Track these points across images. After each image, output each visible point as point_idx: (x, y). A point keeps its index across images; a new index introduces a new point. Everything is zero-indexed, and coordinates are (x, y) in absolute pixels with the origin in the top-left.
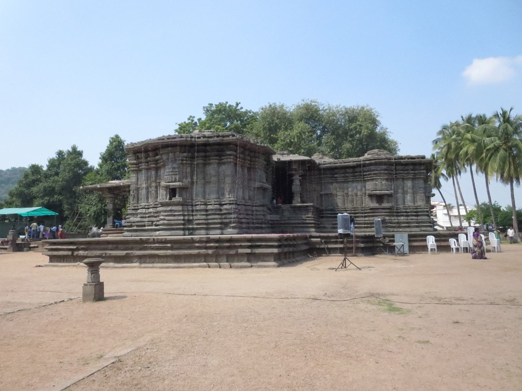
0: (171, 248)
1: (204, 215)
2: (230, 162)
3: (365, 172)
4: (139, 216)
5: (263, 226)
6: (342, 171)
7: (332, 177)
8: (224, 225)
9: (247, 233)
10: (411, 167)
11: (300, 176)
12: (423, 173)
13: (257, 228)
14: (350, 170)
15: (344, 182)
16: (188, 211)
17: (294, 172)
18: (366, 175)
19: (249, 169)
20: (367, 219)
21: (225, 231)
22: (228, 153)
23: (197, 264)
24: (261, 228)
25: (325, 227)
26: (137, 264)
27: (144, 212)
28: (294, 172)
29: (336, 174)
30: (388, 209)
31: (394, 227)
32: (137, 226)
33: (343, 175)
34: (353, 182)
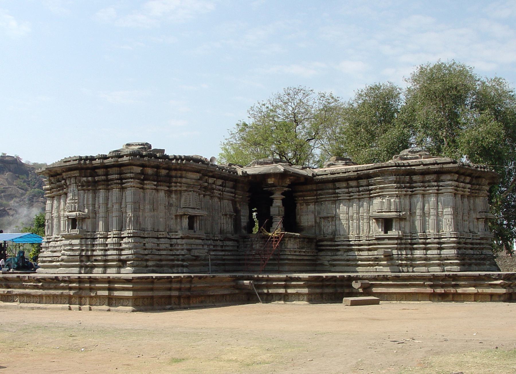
0: (42, 288)
1: (102, 250)
3: (372, 185)
4: (50, 250)
5: (185, 263)
6: (344, 184)
8: (122, 263)
11: (282, 194)
13: (178, 266)
16: (87, 245)
18: (372, 190)
20: (370, 253)
21: (123, 270)
24: (183, 266)
25: (322, 264)
29: (339, 188)
30: (397, 239)
33: (346, 190)
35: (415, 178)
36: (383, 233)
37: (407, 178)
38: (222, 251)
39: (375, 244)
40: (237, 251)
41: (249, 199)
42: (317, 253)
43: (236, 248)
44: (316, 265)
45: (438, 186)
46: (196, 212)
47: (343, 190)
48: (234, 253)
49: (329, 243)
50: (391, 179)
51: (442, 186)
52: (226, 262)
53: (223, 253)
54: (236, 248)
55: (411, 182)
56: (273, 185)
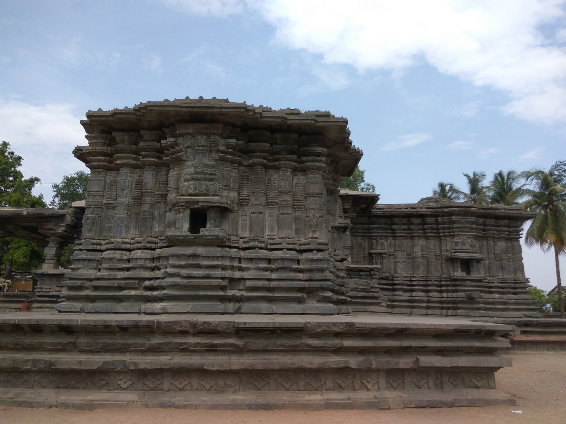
2: (319, 169)
6: (405, 221)
7: (387, 229)
10: (506, 222)
14: (417, 221)
15: (405, 237)
22: (320, 149)
23: (316, 397)
26: (131, 396)
27: (118, 256)
31: (448, 308)
32: (96, 288)
33: (406, 227)
34: (419, 237)
35: (489, 221)
37: (481, 220)
39: (448, 286)
47: (403, 226)
55: (484, 224)
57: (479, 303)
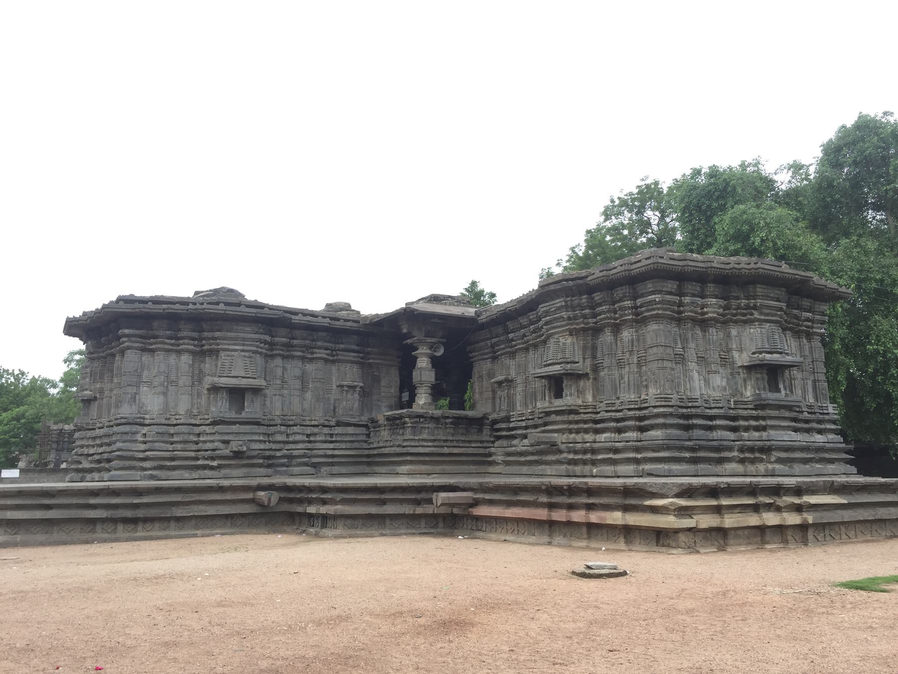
9: (152, 477)
12: (654, 302)
13: (205, 467)
17: (409, 341)
19: (201, 354)
24: (212, 468)
28: (409, 341)
30: (571, 412)
35: (597, 297)
36: (547, 404)
37: (584, 299)
38: (331, 442)
40: (366, 442)
41: (400, 360)
42: (493, 442)
43: (364, 438)
44: (491, 463)
45: (636, 307)
46: (244, 382)
48: (356, 445)
49: (503, 426)
50: (559, 305)
51: (641, 306)
52: (335, 460)
53: (332, 446)
54: (364, 438)
56: (409, 336)
57: (561, 452)
